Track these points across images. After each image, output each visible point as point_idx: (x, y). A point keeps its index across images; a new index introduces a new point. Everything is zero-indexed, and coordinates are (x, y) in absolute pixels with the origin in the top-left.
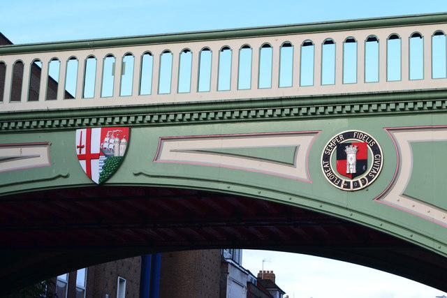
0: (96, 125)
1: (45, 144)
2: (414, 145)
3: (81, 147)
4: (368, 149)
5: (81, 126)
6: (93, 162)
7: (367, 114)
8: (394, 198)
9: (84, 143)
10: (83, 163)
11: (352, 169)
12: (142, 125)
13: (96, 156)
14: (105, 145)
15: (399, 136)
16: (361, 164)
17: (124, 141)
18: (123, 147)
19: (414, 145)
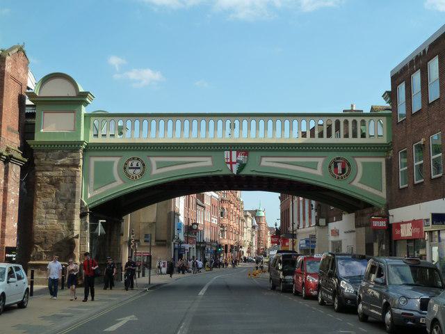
1: (209, 156)
2: (364, 164)
3: (227, 159)
7: (345, 151)
8: (355, 183)
10: (229, 166)
11: (340, 172)
12: (253, 150)
13: (235, 163)
15: (356, 159)
16: (344, 170)
19: (364, 164)
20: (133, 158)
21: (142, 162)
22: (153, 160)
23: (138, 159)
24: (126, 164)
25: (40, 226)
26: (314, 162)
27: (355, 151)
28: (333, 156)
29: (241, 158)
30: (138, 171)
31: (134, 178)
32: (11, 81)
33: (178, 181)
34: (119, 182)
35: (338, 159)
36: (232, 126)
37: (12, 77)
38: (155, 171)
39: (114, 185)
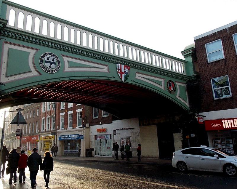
4: (174, 85)
5: (118, 63)
9: (119, 68)
10: (119, 74)
11: (172, 89)
13: (123, 73)
14: (126, 71)
20: (50, 54)
21: (57, 59)
22: (66, 59)
23: (54, 55)
24: (42, 57)
28: (170, 79)
29: (127, 70)
30: (53, 66)
34: (34, 73)
35: (170, 81)
38: (67, 69)
39: (29, 75)
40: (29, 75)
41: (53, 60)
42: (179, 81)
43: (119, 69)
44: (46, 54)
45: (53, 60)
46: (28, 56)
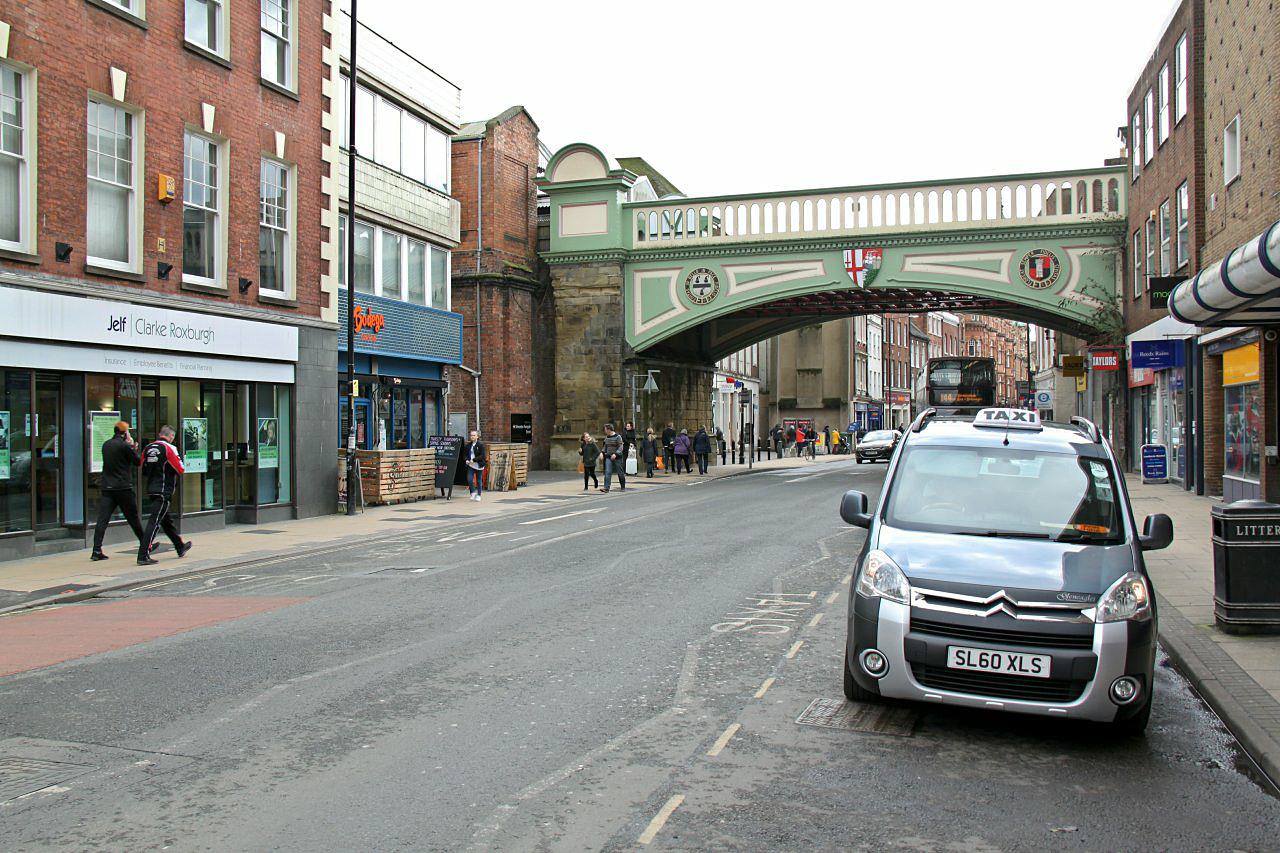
0: (857, 248)
1: (821, 260)
3: (848, 263)
4: (1050, 262)
6: (857, 273)
7: (1049, 238)
9: (850, 260)
10: (851, 274)
12: (891, 246)
13: (860, 269)
14: (866, 261)
15: (1070, 251)
16: (1046, 273)
17: (879, 258)
18: (879, 263)
19: (1081, 257)
22: (731, 271)
24: (689, 280)
25: (566, 382)
26: (995, 261)
27: (1067, 237)
28: (1026, 248)
30: (707, 291)
31: (703, 302)
32: (507, 164)
33: (796, 300)
34: (680, 309)
35: (1036, 252)
36: (856, 207)
37: (507, 157)
38: (734, 290)
39: (673, 314)
40: (673, 314)
41: (706, 281)
42: (1077, 242)
43: (848, 263)
44: (694, 273)
45: (706, 281)
46: (668, 287)
